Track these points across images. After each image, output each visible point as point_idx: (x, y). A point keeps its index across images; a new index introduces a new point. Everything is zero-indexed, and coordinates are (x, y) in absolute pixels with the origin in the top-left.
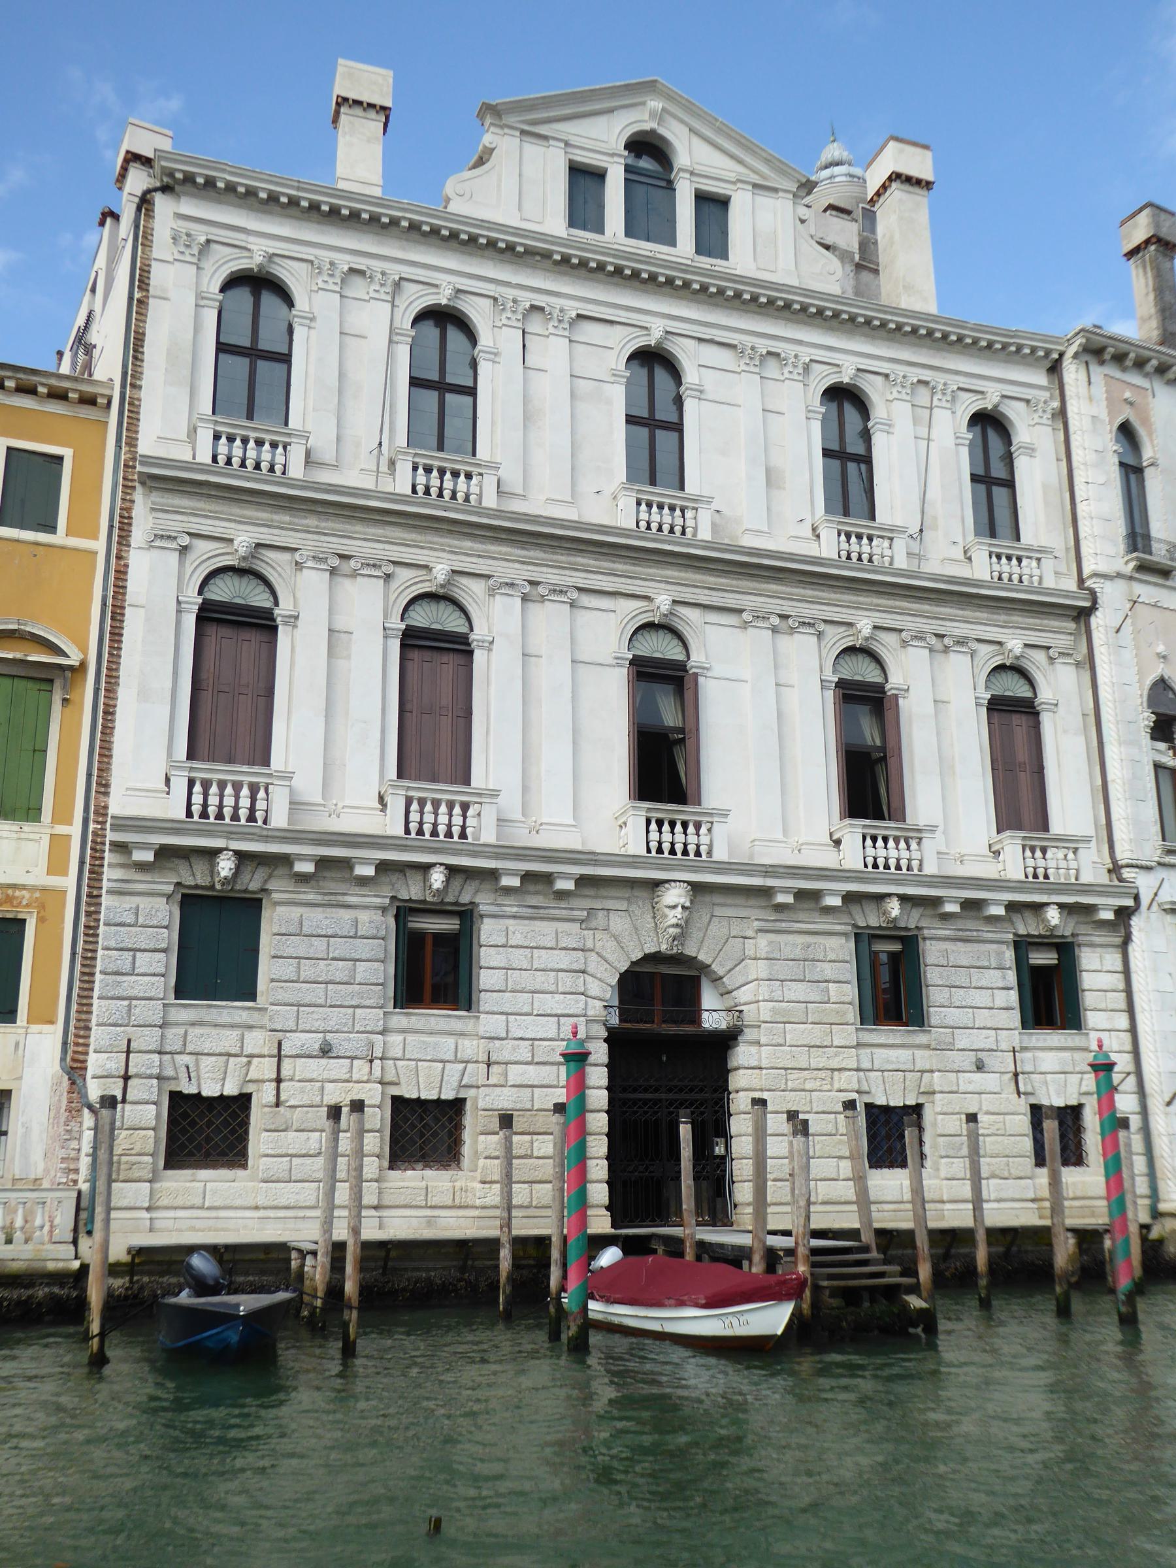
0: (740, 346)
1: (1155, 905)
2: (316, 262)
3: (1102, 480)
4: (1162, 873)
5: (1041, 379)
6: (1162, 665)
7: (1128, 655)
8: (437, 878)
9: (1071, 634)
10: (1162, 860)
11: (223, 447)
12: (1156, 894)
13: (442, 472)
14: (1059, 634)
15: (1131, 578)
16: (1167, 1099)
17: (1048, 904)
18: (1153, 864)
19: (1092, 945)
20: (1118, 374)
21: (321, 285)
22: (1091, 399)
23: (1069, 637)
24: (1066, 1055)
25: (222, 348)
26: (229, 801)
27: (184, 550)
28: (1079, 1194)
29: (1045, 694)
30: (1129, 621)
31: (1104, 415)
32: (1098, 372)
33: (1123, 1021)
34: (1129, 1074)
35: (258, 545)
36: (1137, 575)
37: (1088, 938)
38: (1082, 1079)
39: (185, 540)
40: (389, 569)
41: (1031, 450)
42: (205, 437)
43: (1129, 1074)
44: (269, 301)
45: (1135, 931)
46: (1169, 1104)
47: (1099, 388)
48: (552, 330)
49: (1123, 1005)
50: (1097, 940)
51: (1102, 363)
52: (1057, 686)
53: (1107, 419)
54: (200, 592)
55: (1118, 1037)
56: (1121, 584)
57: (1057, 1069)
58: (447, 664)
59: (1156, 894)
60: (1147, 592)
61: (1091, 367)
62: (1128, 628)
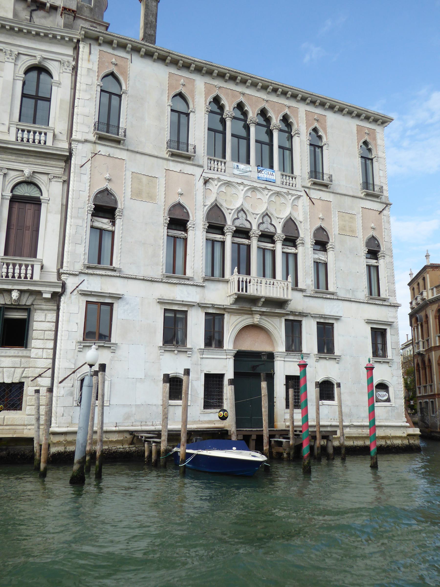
0: (4, 50)
1: (76, 291)
2: (62, 61)
3: (88, 97)
4: (82, 277)
5: (70, 52)
6: (107, 183)
7: (86, 178)
8: (15, 295)
9: (62, 168)
10: (83, 271)
11: (37, 137)
12: (77, 287)
13: (35, 133)
14: (56, 168)
15: (95, 143)
16: (60, 380)
17: (13, 290)
18: (77, 273)
19: (41, 309)
20: (110, 50)
21: (64, 70)
22: (89, 61)
23: (61, 170)
24: (18, 360)
25: (24, 95)
26: (23, 271)
27: (5, 175)
28: (9, 423)
29: (45, 196)
30: (90, 162)
31: (96, 68)
32: (96, 49)
33: (51, 344)
34: (50, 369)
35: (34, 172)
36: (99, 142)
37: (39, 306)
38: (24, 371)
39: (6, 171)
40: (6, 171)
41: (59, 84)
42: (13, 130)
43: (50, 369)
44: (43, 76)
45: (62, 304)
46: (60, 382)
47: (95, 56)
48: (6, 60)
49: (53, 338)
50: (44, 307)
51: (100, 45)
52: (51, 192)
53: (97, 70)
54: (12, 191)
55: (47, 352)
56: (89, 146)
57: (11, 366)
58: (30, 209)
59: (77, 287)
60: (104, 149)
61: (92, 47)
62: (88, 165)
